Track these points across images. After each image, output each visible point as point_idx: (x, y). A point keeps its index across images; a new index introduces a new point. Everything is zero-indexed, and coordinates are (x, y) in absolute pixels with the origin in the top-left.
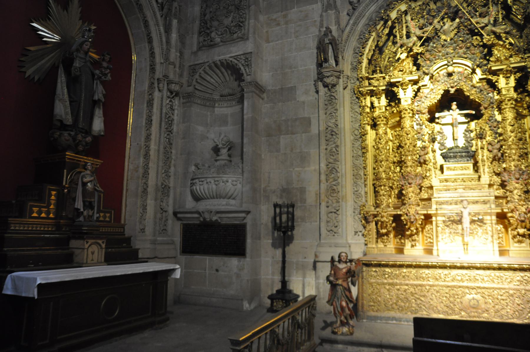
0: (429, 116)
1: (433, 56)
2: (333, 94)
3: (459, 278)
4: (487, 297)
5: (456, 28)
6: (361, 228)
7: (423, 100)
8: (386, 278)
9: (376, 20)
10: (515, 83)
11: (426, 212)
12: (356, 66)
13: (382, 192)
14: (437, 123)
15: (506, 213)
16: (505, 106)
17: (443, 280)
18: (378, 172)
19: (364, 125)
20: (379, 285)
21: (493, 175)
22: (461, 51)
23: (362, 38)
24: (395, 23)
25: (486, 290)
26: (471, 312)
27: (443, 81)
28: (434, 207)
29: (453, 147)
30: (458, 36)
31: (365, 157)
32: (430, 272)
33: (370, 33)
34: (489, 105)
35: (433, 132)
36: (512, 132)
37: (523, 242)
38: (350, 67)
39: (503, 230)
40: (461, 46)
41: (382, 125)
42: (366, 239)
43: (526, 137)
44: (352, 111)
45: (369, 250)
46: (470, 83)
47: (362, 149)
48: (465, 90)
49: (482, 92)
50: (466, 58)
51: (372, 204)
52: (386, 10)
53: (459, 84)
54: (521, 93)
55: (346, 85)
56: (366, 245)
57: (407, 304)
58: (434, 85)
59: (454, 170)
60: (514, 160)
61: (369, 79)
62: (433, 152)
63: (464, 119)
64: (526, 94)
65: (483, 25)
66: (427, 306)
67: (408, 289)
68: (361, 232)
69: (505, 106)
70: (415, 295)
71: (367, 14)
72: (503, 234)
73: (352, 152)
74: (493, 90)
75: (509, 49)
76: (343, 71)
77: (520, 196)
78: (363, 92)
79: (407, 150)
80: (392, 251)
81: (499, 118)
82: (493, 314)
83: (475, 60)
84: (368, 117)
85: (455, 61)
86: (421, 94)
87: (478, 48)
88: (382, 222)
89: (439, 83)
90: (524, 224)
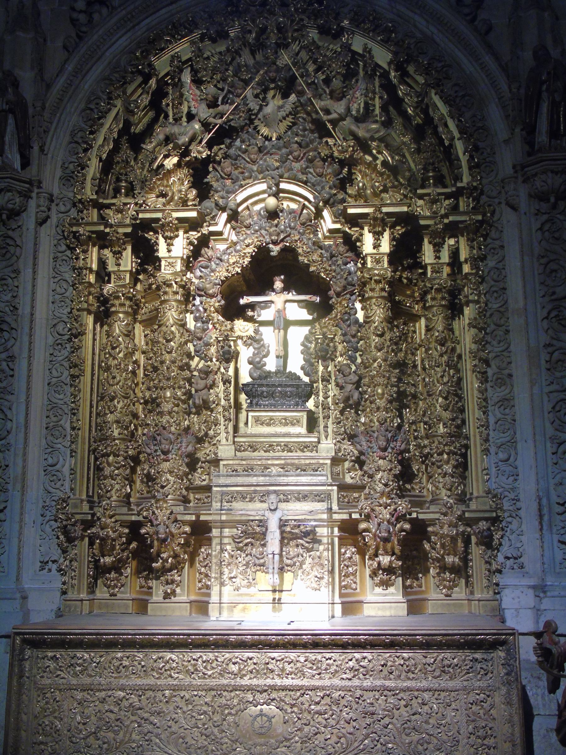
0: (223, 302)
1: (240, 170)
2: (10, 233)
3: (235, 668)
4: (289, 710)
5: (290, 113)
6: (56, 553)
7: (214, 266)
8: (76, 675)
9: (126, 72)
10: (393, 246)
11: (194, 518)
12: (73, 172)
13: (107, 471)
14: (251, 320)
15: (357, 521)
16: (371, 294)
17: (200, 675)
18: (104, 423)
19: (77, 313)
20: (60, 690)
21: (343, 439)
22: (297, 166)
23: (92, 110)
24: (167, 84)
25: (288, 692)
26: (255, 745)
27: (257, 228)
28: (216, 505)
29: (270, 372)
30: (292, 133)
31: (76, 387)
32: (174, 657)
33: (110, 98)
34: (345, 288)
35: (226, 338)
36: (380, 350)
37: (392, 585)
38: (59, 173)
39: (357, 558)
40: (296, 154)
41: (121, 315)
42: (65, 579)
43: (415, 361)
44: (54, 277)
45: (70, 607)
46: (312, 236)
47: (70, 368)
48: (300, 251)
49: (334, 259)
50: (305, 183)
51: (84, 497)
52: (146, 54)
53: (289, 236)
54: (411, 268)
55: (44, 215)
56: (64, 593)
57: (121, 734)
58: (237, 234)
59: (269, 425)
60: (378, 409)
61: (101, 207)
62: (224, 384)
63: (304, 315)
64: (420, 271)
65: (334, 116)
66: (162, 736)
67: (124, 697)
68: (54, 562)
69: (371, 294)
70: (139, 712)
71: (107, 54)
72: (355, 568)
73: (47, 372)
74: (354, 257)
75: (382, 174)
76: (40, 182)
77: (386, 485)
78: (80, 235)
79: (164, 377)
80: (127, 606)
81: (360, 315)
82: (299, 744)
83: (323, 188)
84: (90, 293)
85: (283, 186)
86: (210, 253)
87: (330, 164)
88: (102, 539)
89: (248, 232)
90: (389, 545)
